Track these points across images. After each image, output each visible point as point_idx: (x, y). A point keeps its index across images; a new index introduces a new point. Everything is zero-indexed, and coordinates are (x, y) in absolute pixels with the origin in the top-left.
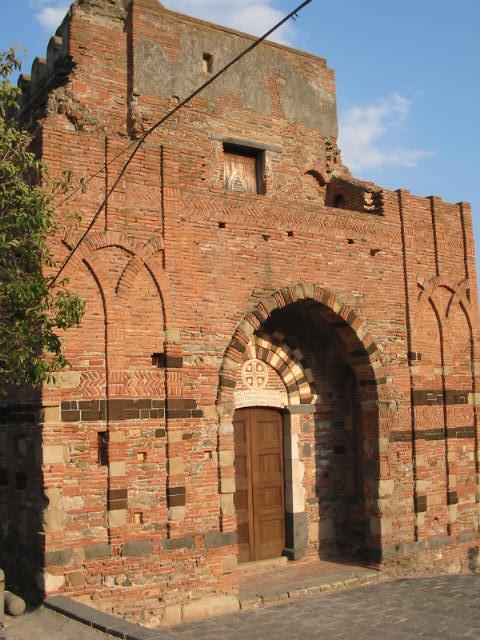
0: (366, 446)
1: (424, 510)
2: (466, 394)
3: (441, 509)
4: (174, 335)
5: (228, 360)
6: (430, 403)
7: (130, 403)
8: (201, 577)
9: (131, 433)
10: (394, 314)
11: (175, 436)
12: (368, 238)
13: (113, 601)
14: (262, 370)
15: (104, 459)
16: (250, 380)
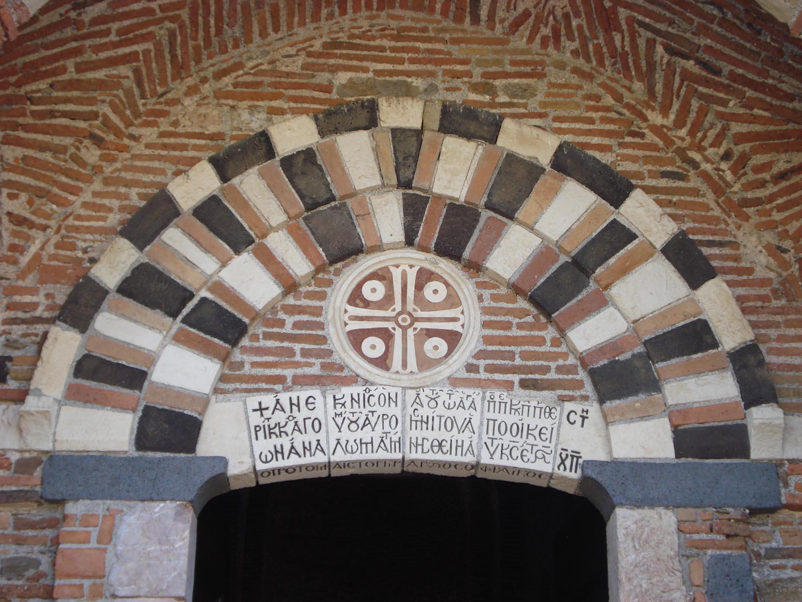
14: (452, 300)
16: (374, 347)
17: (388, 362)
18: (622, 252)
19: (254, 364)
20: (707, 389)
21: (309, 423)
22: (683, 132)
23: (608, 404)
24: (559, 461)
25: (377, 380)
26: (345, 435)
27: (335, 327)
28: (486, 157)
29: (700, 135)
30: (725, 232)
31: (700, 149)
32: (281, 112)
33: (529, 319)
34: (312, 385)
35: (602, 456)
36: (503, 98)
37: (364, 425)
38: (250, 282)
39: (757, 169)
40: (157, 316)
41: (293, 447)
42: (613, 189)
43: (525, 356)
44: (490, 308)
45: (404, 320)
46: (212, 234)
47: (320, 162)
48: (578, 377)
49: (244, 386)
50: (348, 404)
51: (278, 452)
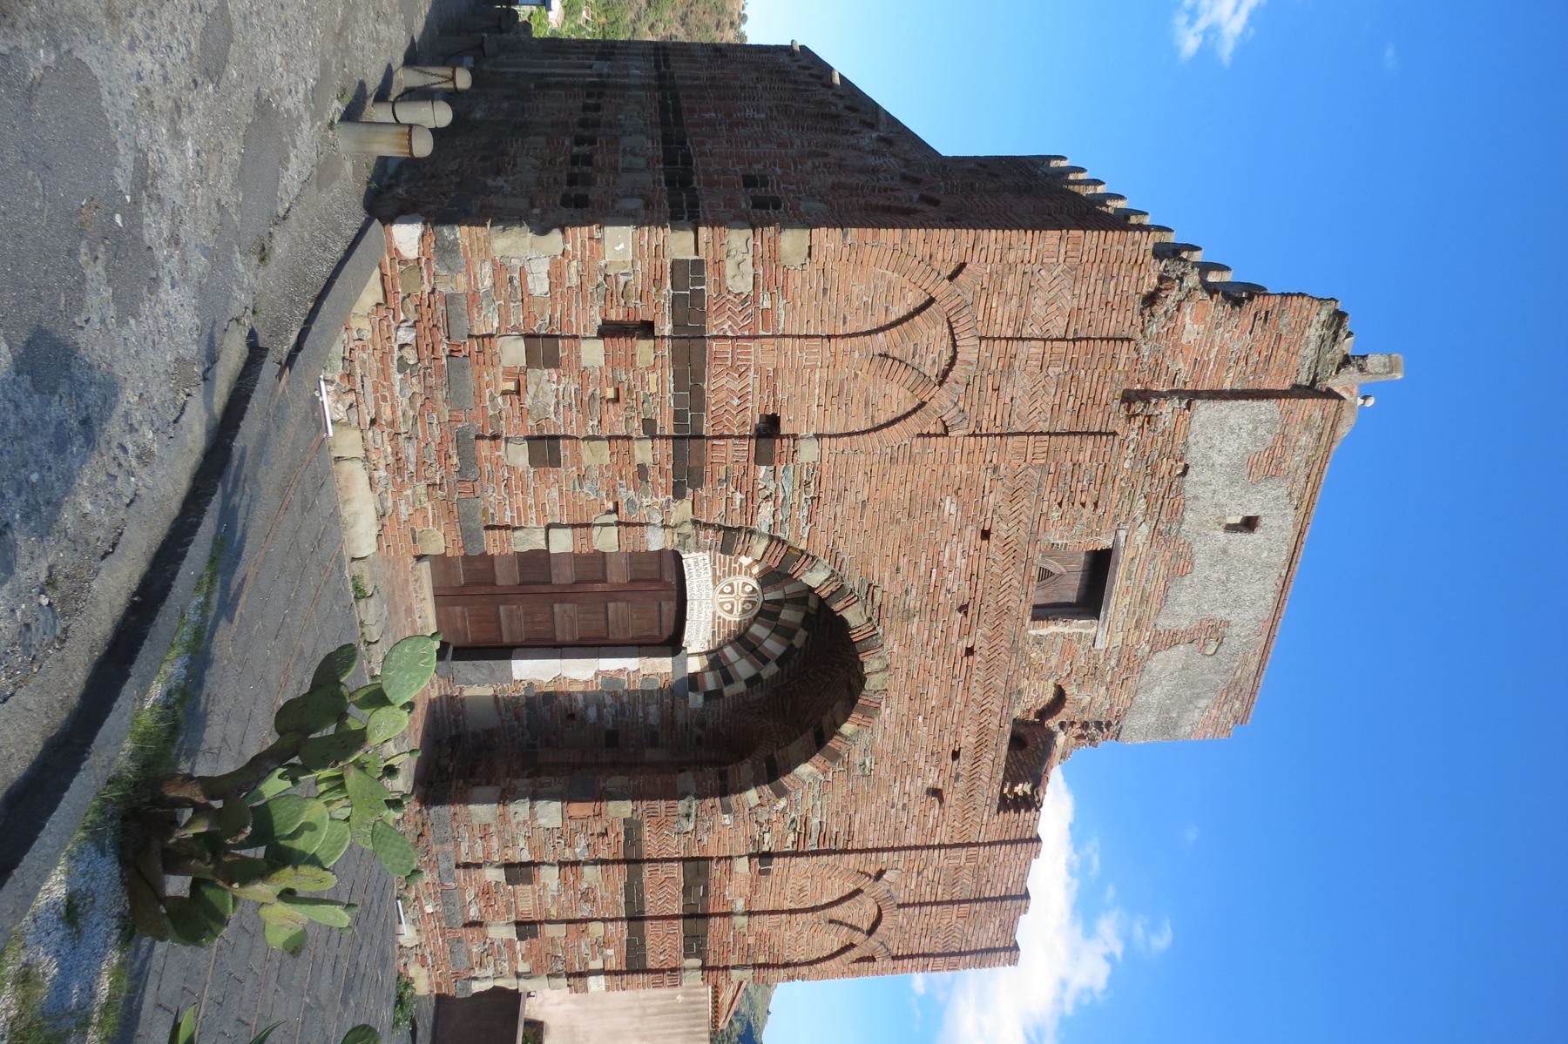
0: (617, 781)
1: (509, 881)
2: (700, 954)
3: (509, 911)
4: (808, 452)
5: (765, 542)
6: (687, 890)
7: (699, 376)
8: (409, 492)
9: (652, 378)
10: (835, 830)
11: (644, 452)
12: (961, 785)
13: (373, 341)
15: (609, 330)
42: (780, 661)
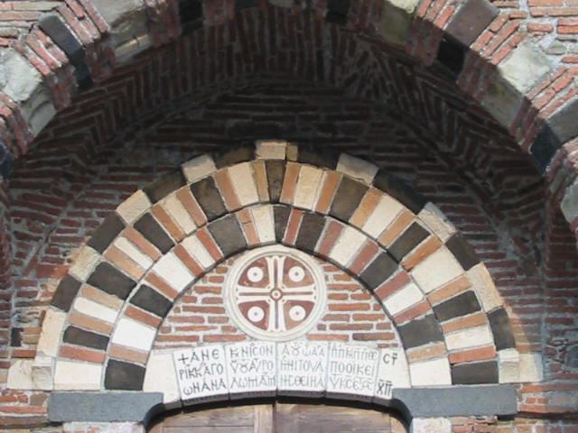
14: (308, 280)
16: (256, 314)
17: (266, 324)
18: (420, 245)
19: (177, 329)
20: (472, 338)
21: (215, 367)
22: (462, 157)
23: (410, 350)
24: (378, 388)
25: (259, 337)
26: (239, 375)
27: (230, 300)
28: (329, 179)
29: (472, 160)
30: (490, 228)
31: (473, 169)
32: (189, 150)
33: (359, 292)
34: (216, 341)
35: (407, 386)
36: (341, 136)
37: (251, 368)
38: (172, 272)
39: (510, 185)
40: (114, 299)
41: (205, 384)
43: (357, 317)
44: (333, 285)
45: (276, 294)
46: (147, 241)
47: (217, 186)
48: (391, 331)
49: (172, 343)
50: (240, 355)
51: (195, 387)
